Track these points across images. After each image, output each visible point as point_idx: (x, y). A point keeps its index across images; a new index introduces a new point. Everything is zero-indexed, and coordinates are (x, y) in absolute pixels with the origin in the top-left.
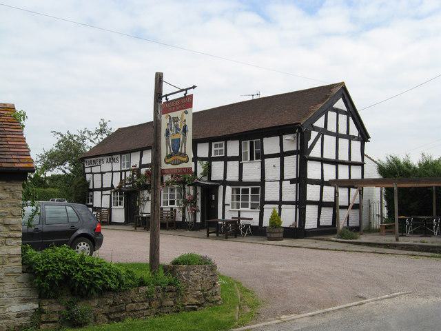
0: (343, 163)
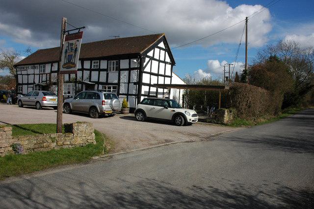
0: (161, 75)
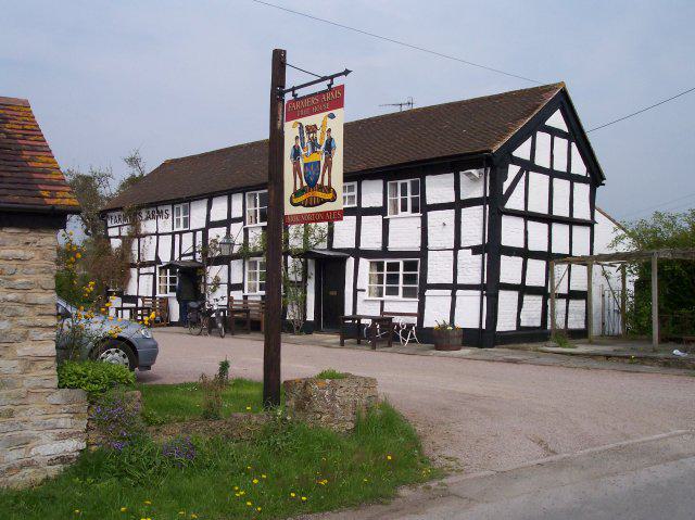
0: (561, 220)
